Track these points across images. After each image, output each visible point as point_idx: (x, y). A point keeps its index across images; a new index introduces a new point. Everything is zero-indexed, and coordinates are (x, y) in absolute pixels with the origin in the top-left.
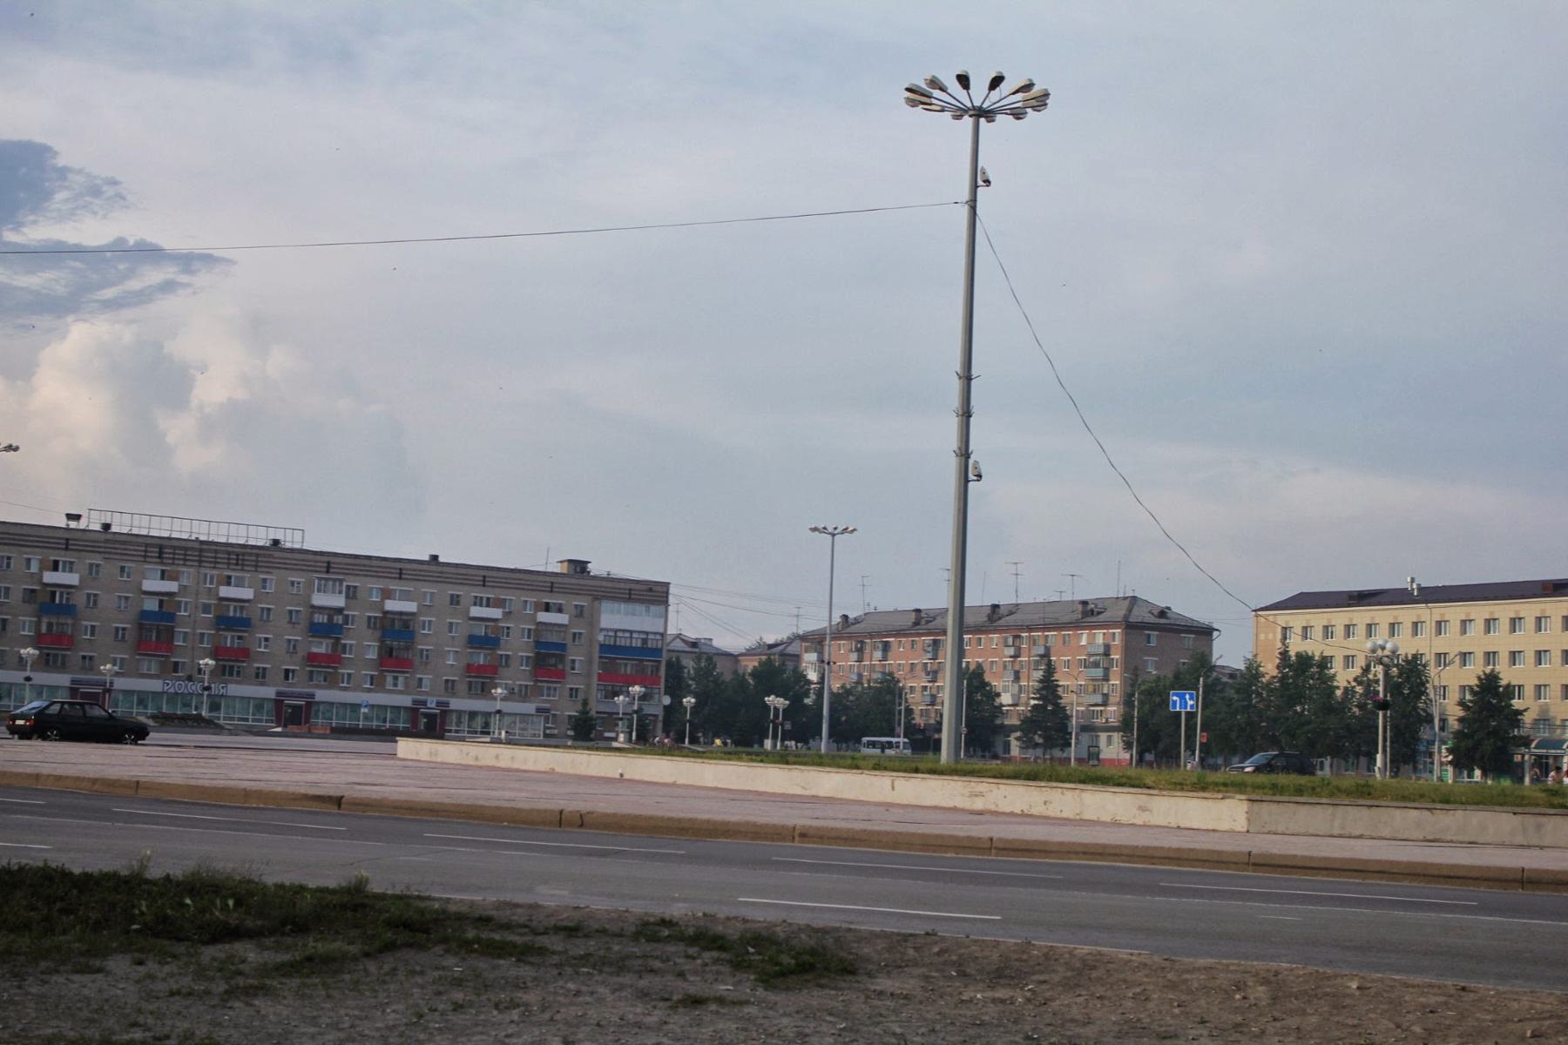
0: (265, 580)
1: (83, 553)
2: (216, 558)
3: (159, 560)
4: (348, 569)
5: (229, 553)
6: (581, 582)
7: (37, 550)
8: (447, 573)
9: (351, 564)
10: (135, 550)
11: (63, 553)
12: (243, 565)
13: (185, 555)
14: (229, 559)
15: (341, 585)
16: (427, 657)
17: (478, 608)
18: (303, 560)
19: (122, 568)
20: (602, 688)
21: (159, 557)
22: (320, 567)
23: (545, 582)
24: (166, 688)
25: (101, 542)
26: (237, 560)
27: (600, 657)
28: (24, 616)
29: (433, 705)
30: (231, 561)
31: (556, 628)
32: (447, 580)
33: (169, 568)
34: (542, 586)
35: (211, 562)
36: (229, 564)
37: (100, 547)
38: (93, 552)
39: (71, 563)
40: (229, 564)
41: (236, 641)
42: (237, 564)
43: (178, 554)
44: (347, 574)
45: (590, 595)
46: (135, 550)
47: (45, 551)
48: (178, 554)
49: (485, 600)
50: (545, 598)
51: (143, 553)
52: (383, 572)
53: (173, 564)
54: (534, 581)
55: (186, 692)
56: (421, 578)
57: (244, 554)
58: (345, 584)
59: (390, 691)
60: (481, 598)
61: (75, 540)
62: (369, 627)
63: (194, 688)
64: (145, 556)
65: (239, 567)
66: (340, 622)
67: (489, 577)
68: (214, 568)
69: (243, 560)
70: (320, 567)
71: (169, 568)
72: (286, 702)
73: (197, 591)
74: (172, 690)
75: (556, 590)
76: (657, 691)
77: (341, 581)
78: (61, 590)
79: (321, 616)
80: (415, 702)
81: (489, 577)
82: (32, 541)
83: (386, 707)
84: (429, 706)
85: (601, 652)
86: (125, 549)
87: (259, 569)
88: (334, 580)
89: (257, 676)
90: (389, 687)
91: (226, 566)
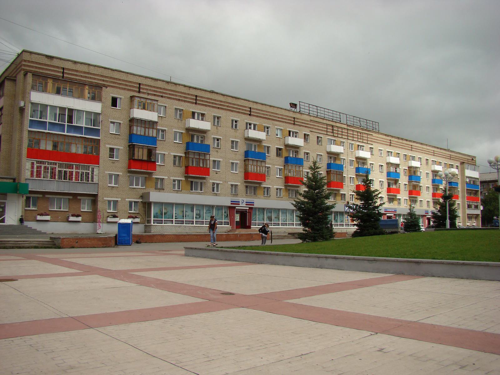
1: (301, 127)
3: (332, 134)
7: (281, 123)
11: (292, 126)
19: (318, 137)
21: (333, 132)
25: (307, 121)
28: (276, 165)
38: (306, 127)
39: (296, 133)
45: (459, 161)
47: (285, 124)
53: (338, 137)
68: (353, 140)
69: (363, 136)
71: (336, 139)
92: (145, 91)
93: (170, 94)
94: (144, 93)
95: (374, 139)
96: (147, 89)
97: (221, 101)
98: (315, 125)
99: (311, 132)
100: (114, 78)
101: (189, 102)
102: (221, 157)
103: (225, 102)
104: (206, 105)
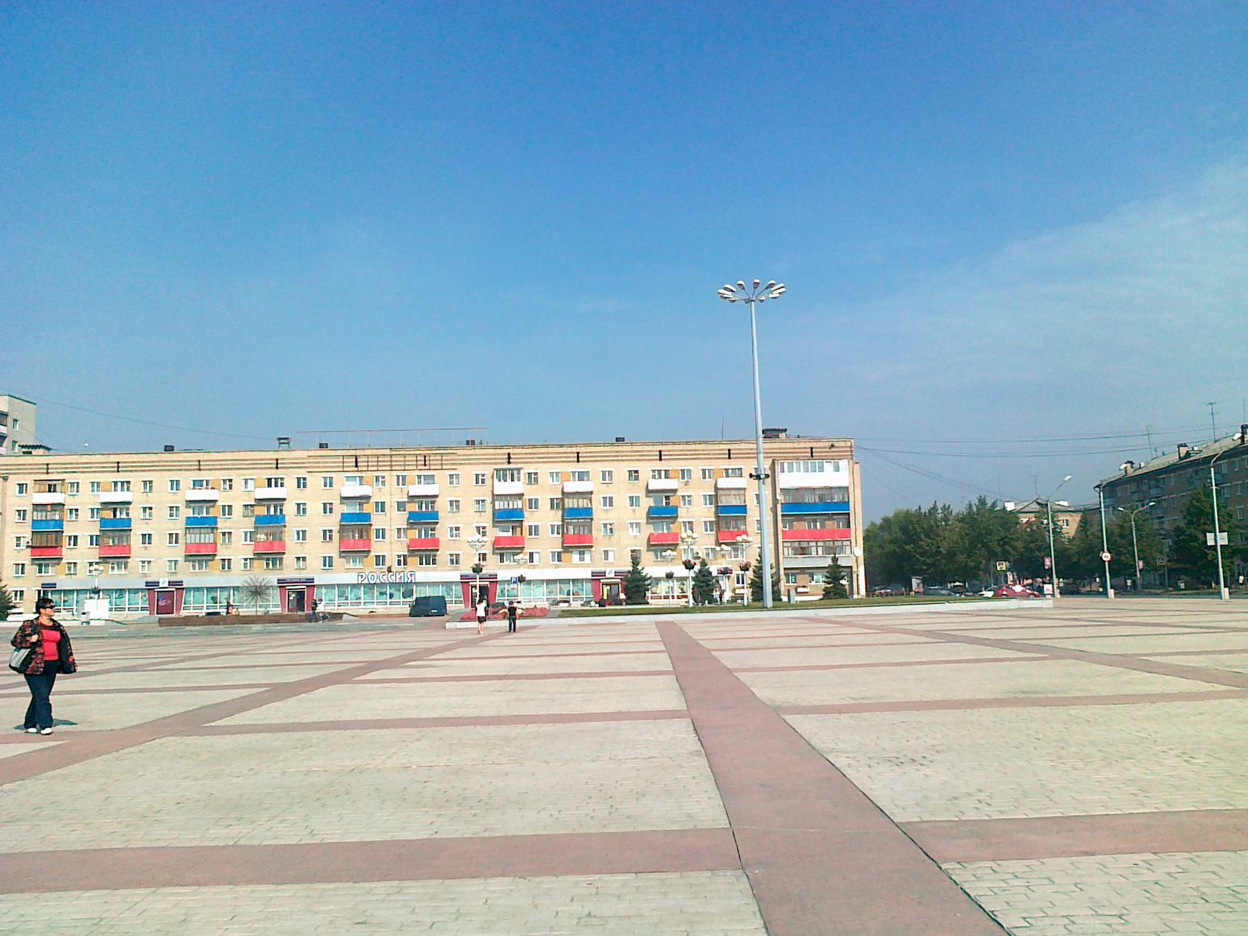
0: (451, 476)
2: (405, 461)
3: (356, 469)
4: (527, 458)
5: (416, 455)
6: (776, 445)
8: (622, 452)
9: (529, 454)
10: (335, 462)
12: (430, 465)
13: (378, 461)
14: (417, 461)
15: (519, 473)
16: (611, 529)
17: (572, 482)
18: (484, 455)
20: (789, 544)
21: (356, 466)
22: (501, 459)
23: (722, 450)
24: (360, 579)
25: (303, 459)
26: (425, 461)
27: (782, 515)
29: (612, 575)
30: (418, 463)
31: (736, 492)
32: (623, 458)
33: (363, 474)
34: (720, 454)
35: (401, 465)
36: (417, 465)
37: (304, 463)
38: (299, 467)
40: (417, 465)
41: (430, 532)
42: (425, 465)
43: (372, 462)
44: (527, 463)
46: (335, 462)
47: (258, 471)
48: (372, 462)
49: (663, 473)
50: (723, 465)
51: (389, 463)
52: (560, 457)
54: (710, 450)
55: (378, 582)
56: (620, 458)
57: (429, 455)
58: (522, 471)
59: (577, 566)
60: (659, 471)
61: (283, 459)
62: (552, 507)
63: (393, 577)
64: (391, 466)
65: (427, 467)
66: (520, 506)
67: (664, 451)
69: (430, 460)
70: (501, 459)
72: (471, 583)
73: (391, 492)
74: (366, 581)
75: (807, 450)
76: (848, 543)
77: (519, 470)
78: (274, 503)
79: (502, 503)
80: (593, 574)
81: (664, 451)
82: (248, 464)
83: (570, 580)
84: (607, 576)
85: (782, 512)
86: (326, 463)
87: (444, 467)
88: (512, 470)
89: (452, 561)
90: (814, 553)
91: (415, 468)
92: (54, 471)
93: (83, 468)
94: (52, 473)
95: (462, 460)
96: (56, 468)
97: (153, 462)
98: (319, 463)
99: (309, 473)
100: (19, 465)
101: (108, 472)
102: (153, 529)
103: (157, 462)
104: (131, 471)
